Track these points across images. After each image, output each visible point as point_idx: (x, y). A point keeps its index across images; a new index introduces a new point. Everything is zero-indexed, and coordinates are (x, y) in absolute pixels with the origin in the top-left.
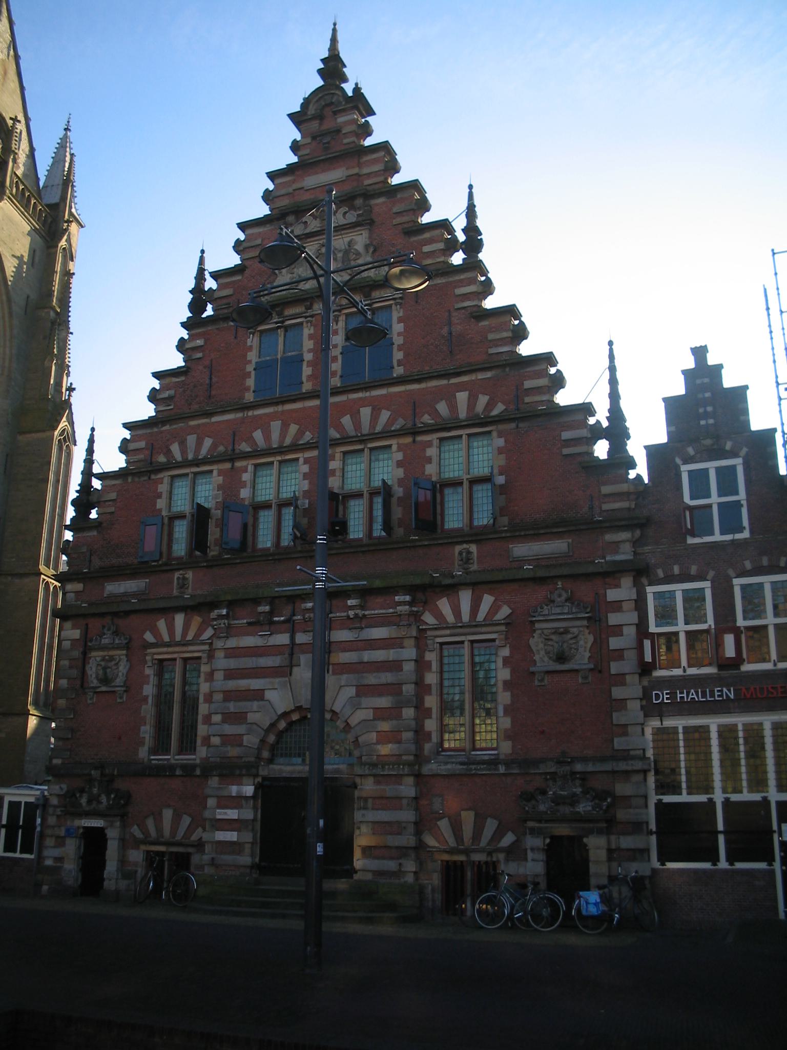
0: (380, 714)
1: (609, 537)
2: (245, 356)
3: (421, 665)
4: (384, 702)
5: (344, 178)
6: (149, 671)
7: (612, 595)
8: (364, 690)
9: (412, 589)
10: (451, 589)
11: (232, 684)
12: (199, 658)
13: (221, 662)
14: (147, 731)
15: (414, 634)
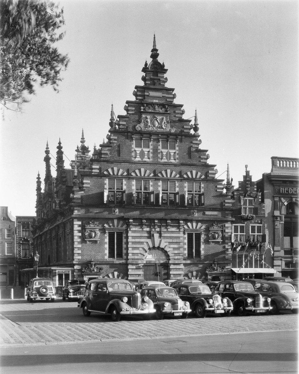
0: (174, 249)
1: (227, 212)
2: (131, 146)
3: (185, 238)
4: (176, 246)
5: (161, 96)
6: (107, 235)
7: (227, 225)
8: (170, 243)
9: (184, 220)
10: (191, 221)
11: (134, 240)
12: (122, 233)
13: (130, 234)
14: (107, 252)
15: (183, 231)
